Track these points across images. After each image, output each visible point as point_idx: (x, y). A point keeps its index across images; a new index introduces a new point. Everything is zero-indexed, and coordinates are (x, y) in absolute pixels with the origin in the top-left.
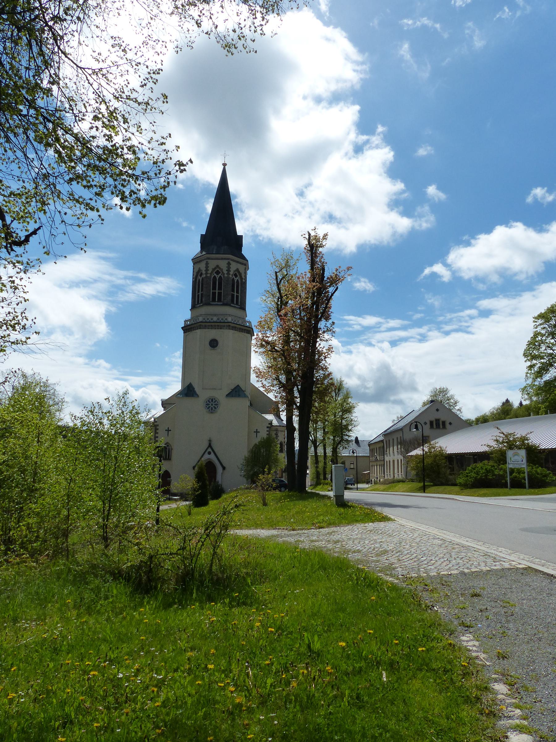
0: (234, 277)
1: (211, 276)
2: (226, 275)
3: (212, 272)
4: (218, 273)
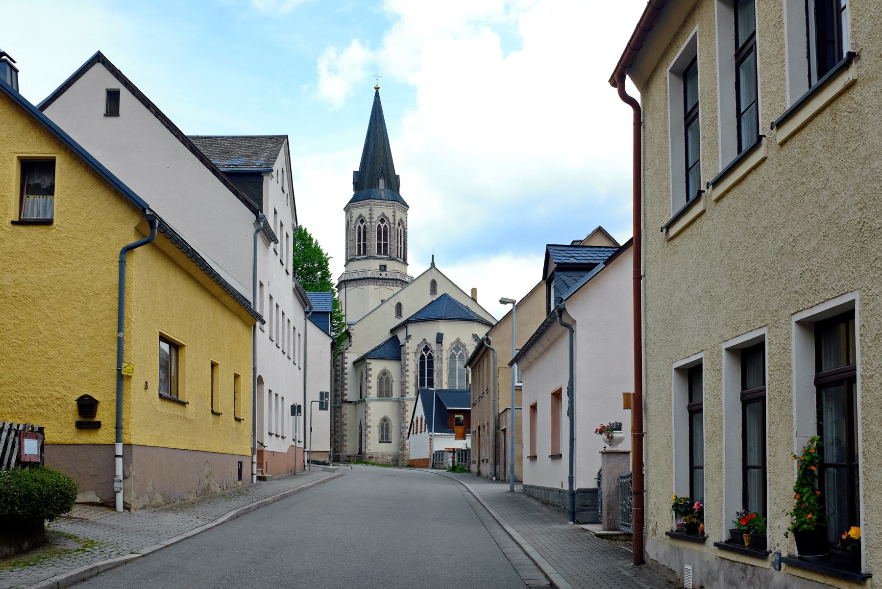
3: (356, 222)
4: (362, 221)
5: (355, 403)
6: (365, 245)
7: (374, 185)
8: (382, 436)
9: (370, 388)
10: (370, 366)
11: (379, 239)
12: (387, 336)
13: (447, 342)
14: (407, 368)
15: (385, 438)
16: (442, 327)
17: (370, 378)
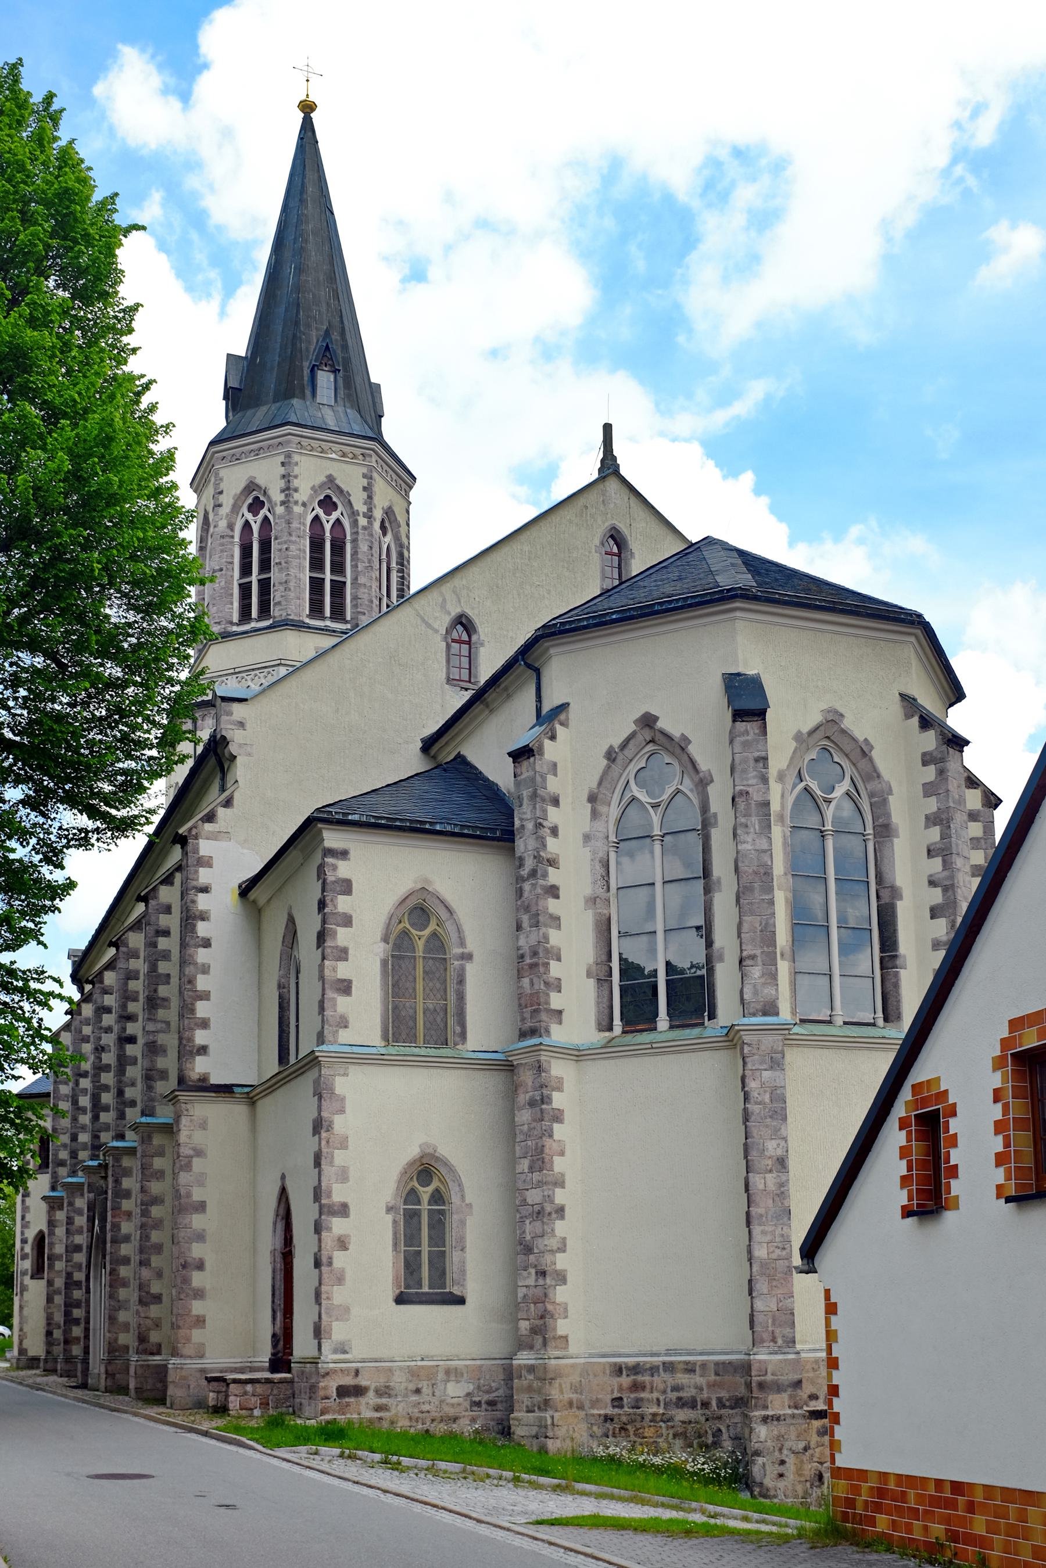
0: (320, 512)
1: (231, 527)
2: (280, 510)
3: (236, 508)
4: (256, 506)
5: (251, 1096)
7: (294, 386)
8: (411, 1266)
9: (345, 987)
10: (343, 869)
11: (317, 564)
12: (410, 762)
13: (788, 717)
14: (554, 876)
15: (425, 1281)
17: (342, 936)
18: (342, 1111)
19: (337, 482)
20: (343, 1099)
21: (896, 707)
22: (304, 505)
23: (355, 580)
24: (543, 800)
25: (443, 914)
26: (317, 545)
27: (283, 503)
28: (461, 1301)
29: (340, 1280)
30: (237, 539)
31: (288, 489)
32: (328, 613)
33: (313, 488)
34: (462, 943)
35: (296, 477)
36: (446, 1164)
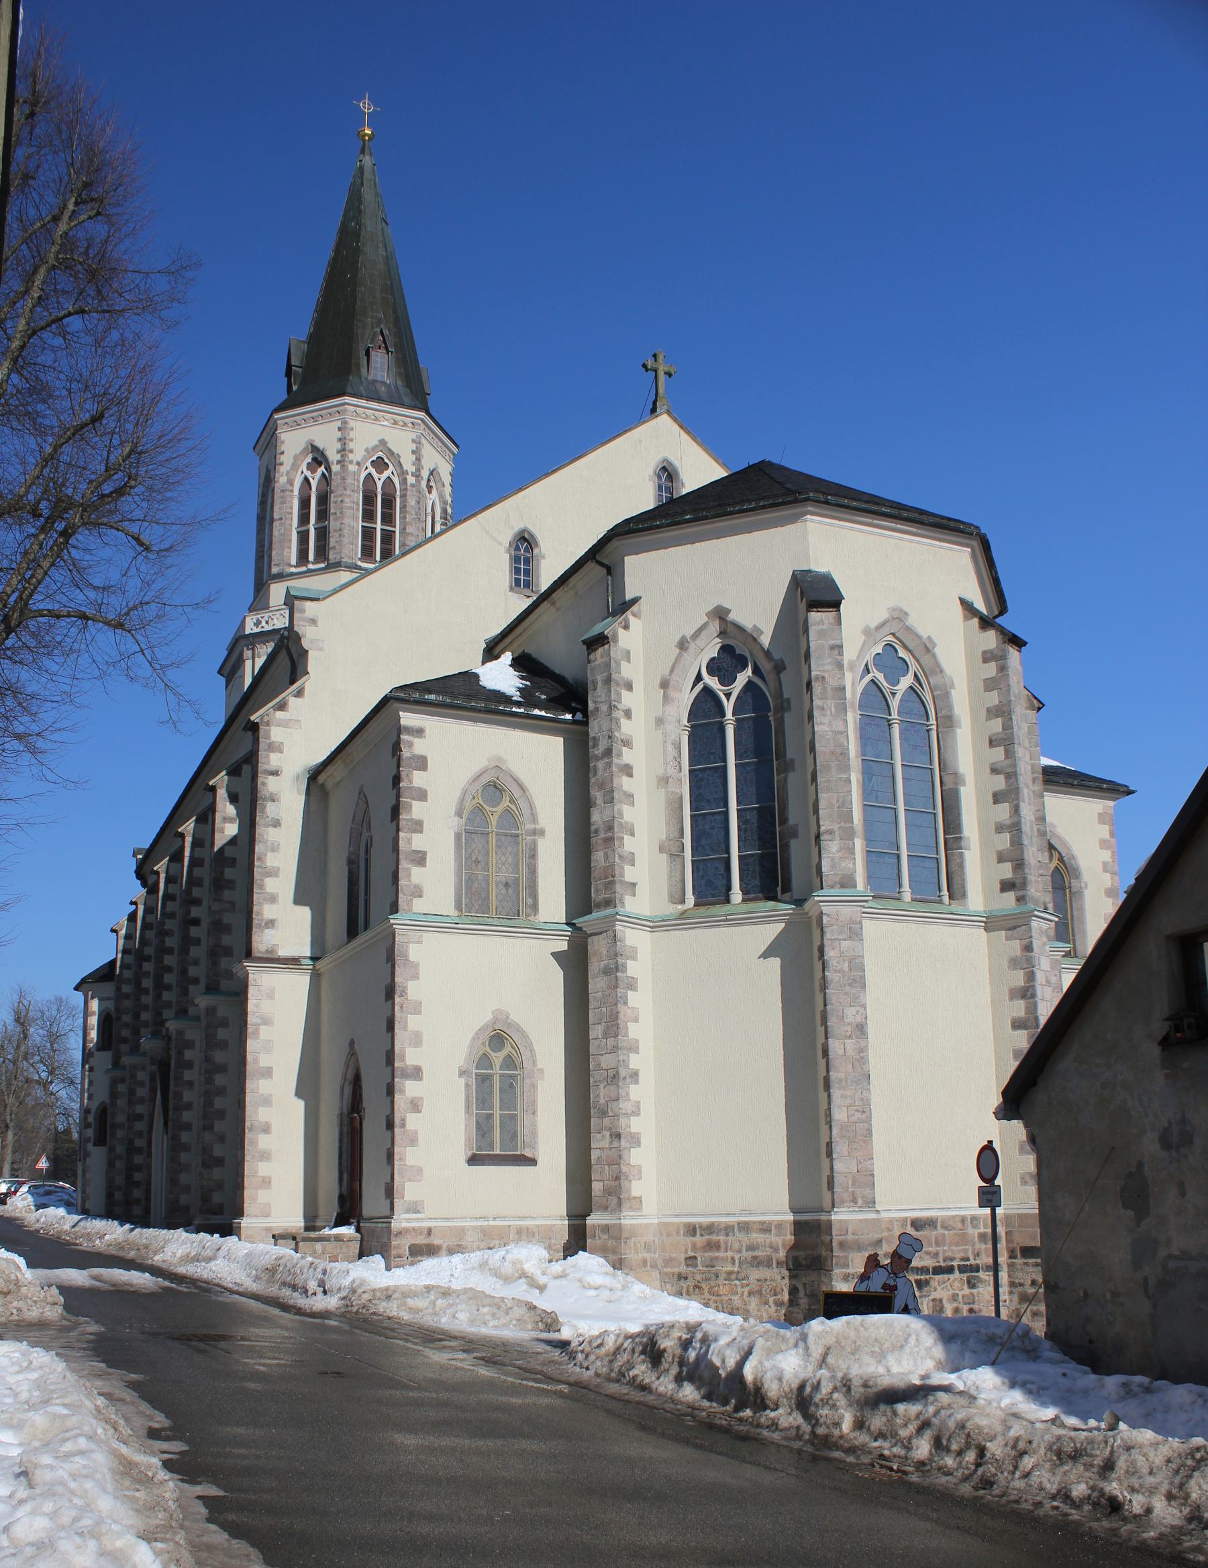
1: (291, 482)
3: (295, 467)
6: (323, 534)
8: (483, 1128)
11: (368, 515)
16: (824, 541)
18: (416, 977)
19: (390, 445)
20: (416, 966)
21: (958, 610)
22: (358, 464)
23: (403, 530)
24: (618, 684)
25: (517, 793)
26: (369, 499)
27: (339, 462)
28: (532, 1162)
29: (413, 1141)
30: (296, 492)
31: (344, 450)
32: (378, 558)
33: (367, 450)
34: (534, 819)
35: (351, 440)
36: (518, 1029)
